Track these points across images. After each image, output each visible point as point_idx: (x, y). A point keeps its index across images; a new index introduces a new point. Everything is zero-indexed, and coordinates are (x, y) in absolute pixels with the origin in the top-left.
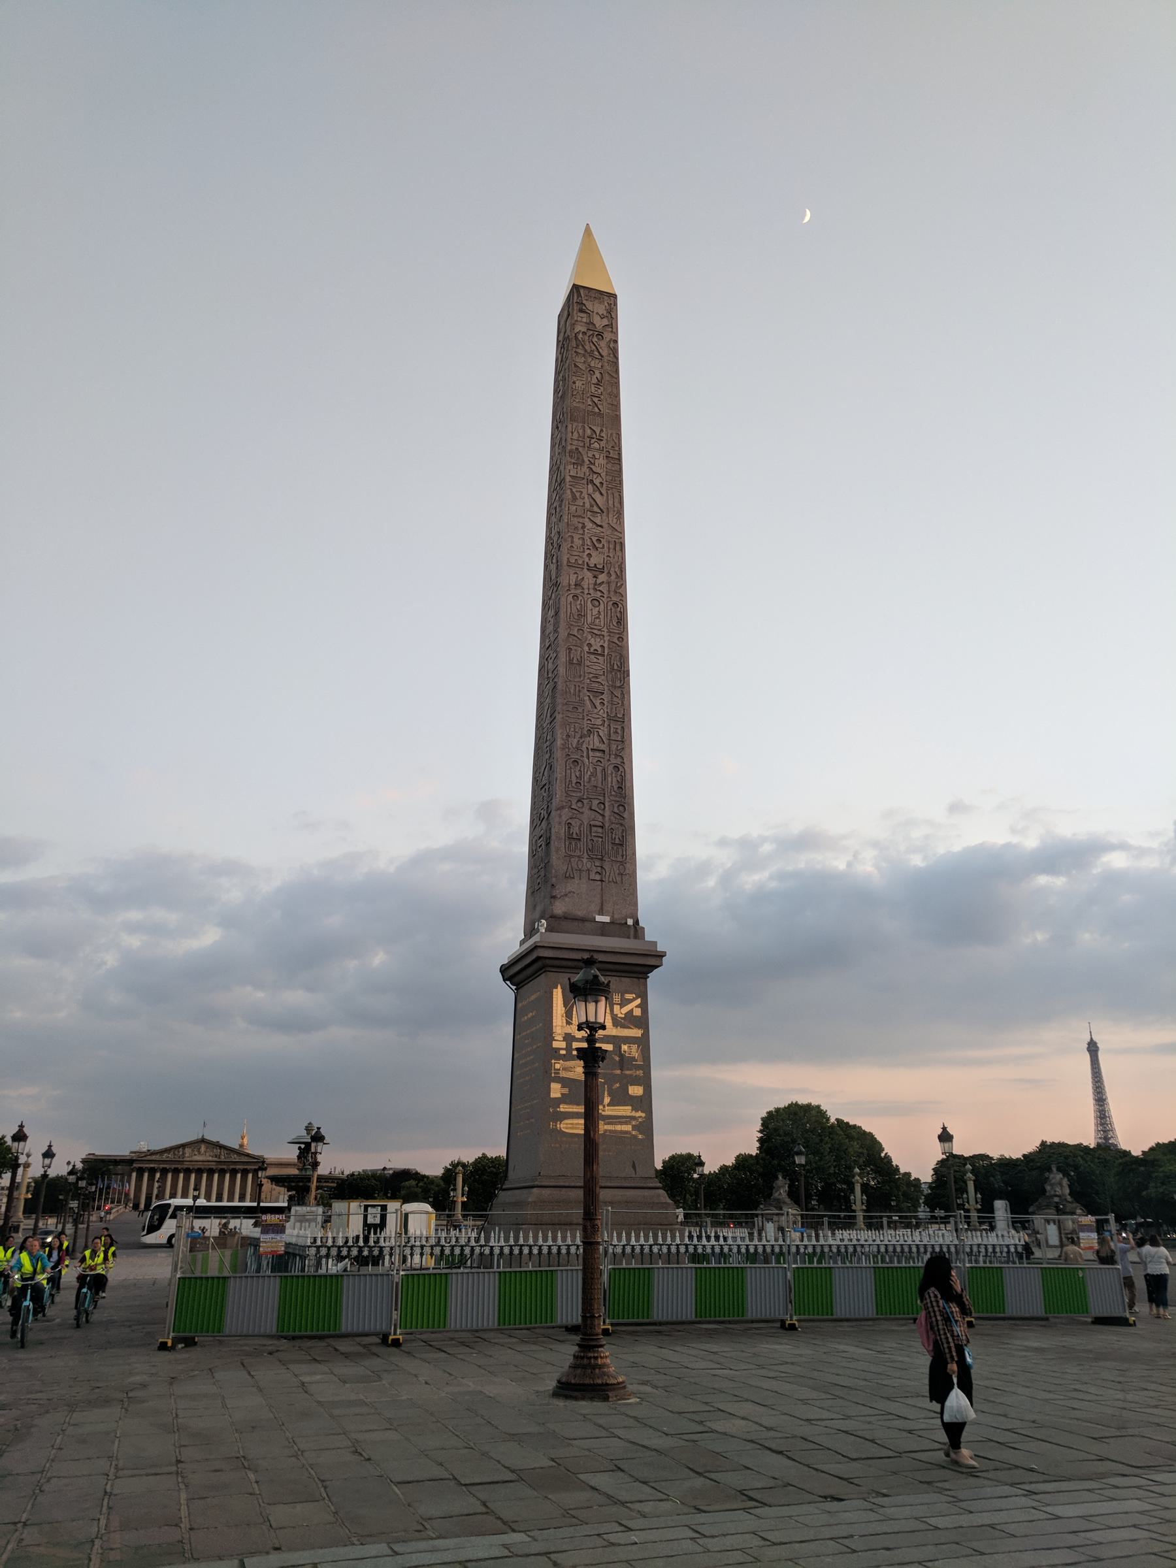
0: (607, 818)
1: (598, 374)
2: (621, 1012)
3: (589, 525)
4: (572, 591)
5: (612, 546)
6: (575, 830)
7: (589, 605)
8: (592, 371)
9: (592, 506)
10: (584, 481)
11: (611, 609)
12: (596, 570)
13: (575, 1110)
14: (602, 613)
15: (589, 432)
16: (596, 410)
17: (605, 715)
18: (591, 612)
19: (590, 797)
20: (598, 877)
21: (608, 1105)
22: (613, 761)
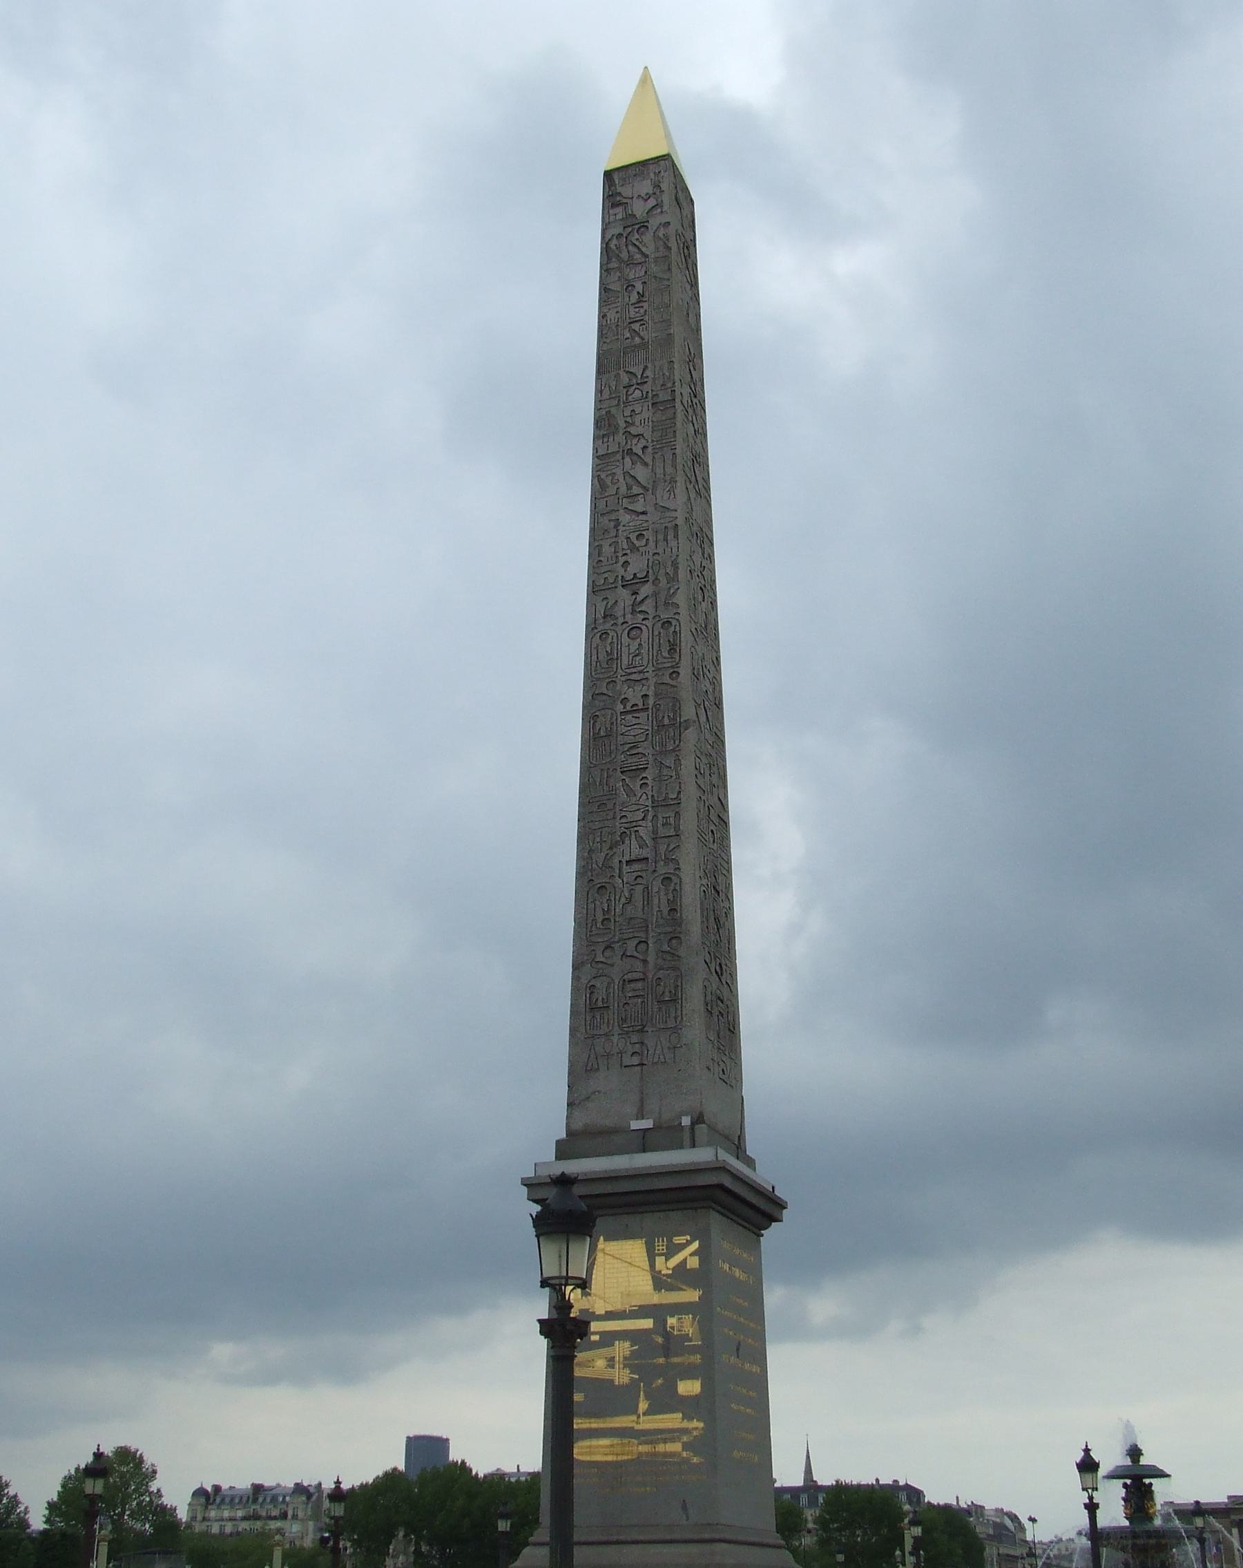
0: (651, 966)
1: (639, 287)
2: (665, 1266)
3: (625, 518)
4: (600, 628)
5: (661, 537)
6: (600, 995)
7: (625, 640)
8: (630, 286)
9: (629, 488)
10: (619, 457)
11: (660, 633)
12: (632, 585)
13: (594, 1426)
14: (645, 645)
15: (625, 379)
16: (637, 340)
17: (649, 803)
18: (628, 646)
19: (626, 936)
20: (635, 1060)
21: (644, 1414)
22: (662, 869)
